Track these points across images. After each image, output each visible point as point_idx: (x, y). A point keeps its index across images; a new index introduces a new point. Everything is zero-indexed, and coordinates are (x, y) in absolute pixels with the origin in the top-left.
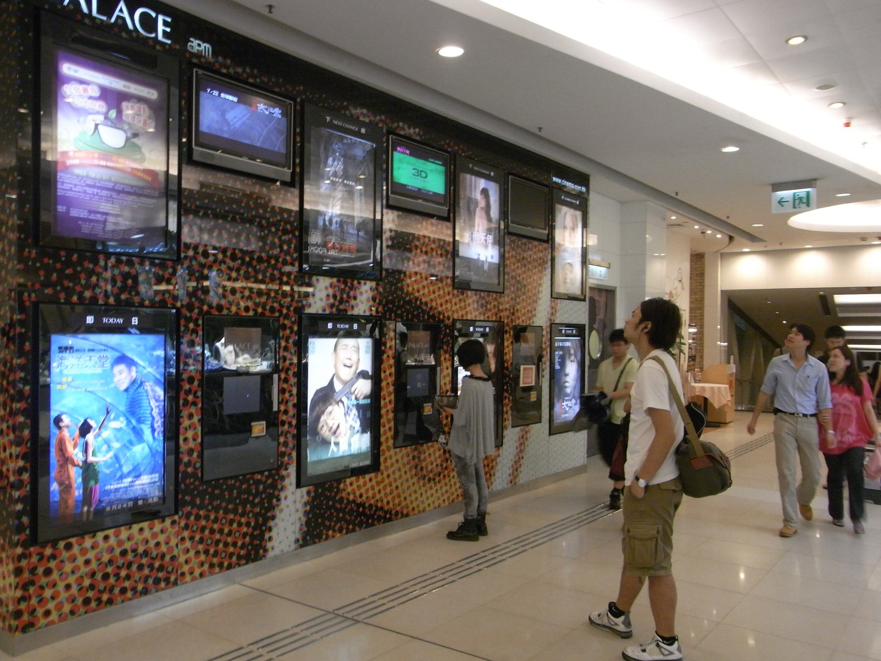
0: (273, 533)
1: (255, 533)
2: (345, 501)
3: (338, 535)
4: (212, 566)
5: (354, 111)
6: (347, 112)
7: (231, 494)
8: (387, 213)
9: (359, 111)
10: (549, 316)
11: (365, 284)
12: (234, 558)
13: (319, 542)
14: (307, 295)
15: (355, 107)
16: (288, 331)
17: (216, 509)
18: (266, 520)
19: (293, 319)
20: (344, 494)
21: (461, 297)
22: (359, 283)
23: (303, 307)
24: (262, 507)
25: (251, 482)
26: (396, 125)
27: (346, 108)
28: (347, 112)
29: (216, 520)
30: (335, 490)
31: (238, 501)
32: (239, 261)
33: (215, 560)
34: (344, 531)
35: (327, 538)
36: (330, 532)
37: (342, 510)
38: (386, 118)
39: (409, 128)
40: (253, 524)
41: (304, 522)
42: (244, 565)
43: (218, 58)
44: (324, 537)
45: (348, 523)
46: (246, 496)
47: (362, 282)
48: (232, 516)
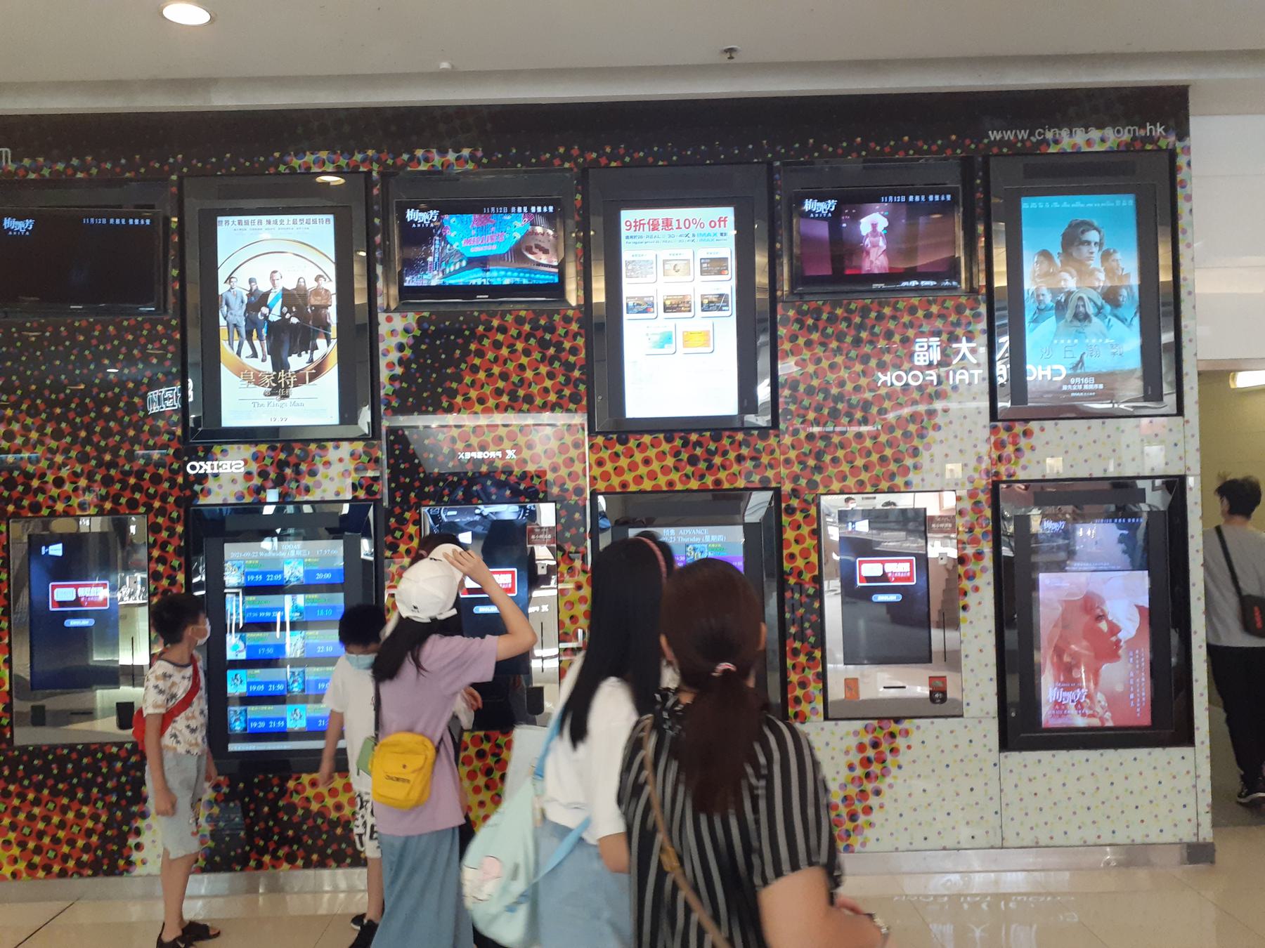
0: (145, 839)
1: (109, 833)
2: (300, 812)
3: (286, 866)
4: (32, 867)
5: (296, 162)
6: (282, 168)
7: (62, 768)
8: (389, 320)
9: (309, 158)
10: (986, 463)
11: (337, 447)
12: (71, 864)
13: (241, 870)
14: (202, 478)
15: (299, 153)
16: (165, 534)
17: (38, 787)
18: (129, 818)
19: (175, 515)
20: (296, 799)
21: (619, 448)
22: (323, 448)
23: (195, 495)
24: (121, 795)
25: (100, 755)
26: (405, 157)
27: (281, 161)
28: (282, 168)
29: (36, 802)
30: (276, 789)
31: (75, 781)
32: (68, 439)
33: (37, 859)
34: (300, 862)
35: (260, 865)
36: (267, 858)
37: (297, 827)
38: (379, 151)
39: (443, 152)
40: (104, 818)
41: (207, 833)
42: (89, 876)
43: (21, 161)
44: (252, 863)
45: (309, 851)
46: (90, 775)
47: (330, 445)
48: (65, 801)
